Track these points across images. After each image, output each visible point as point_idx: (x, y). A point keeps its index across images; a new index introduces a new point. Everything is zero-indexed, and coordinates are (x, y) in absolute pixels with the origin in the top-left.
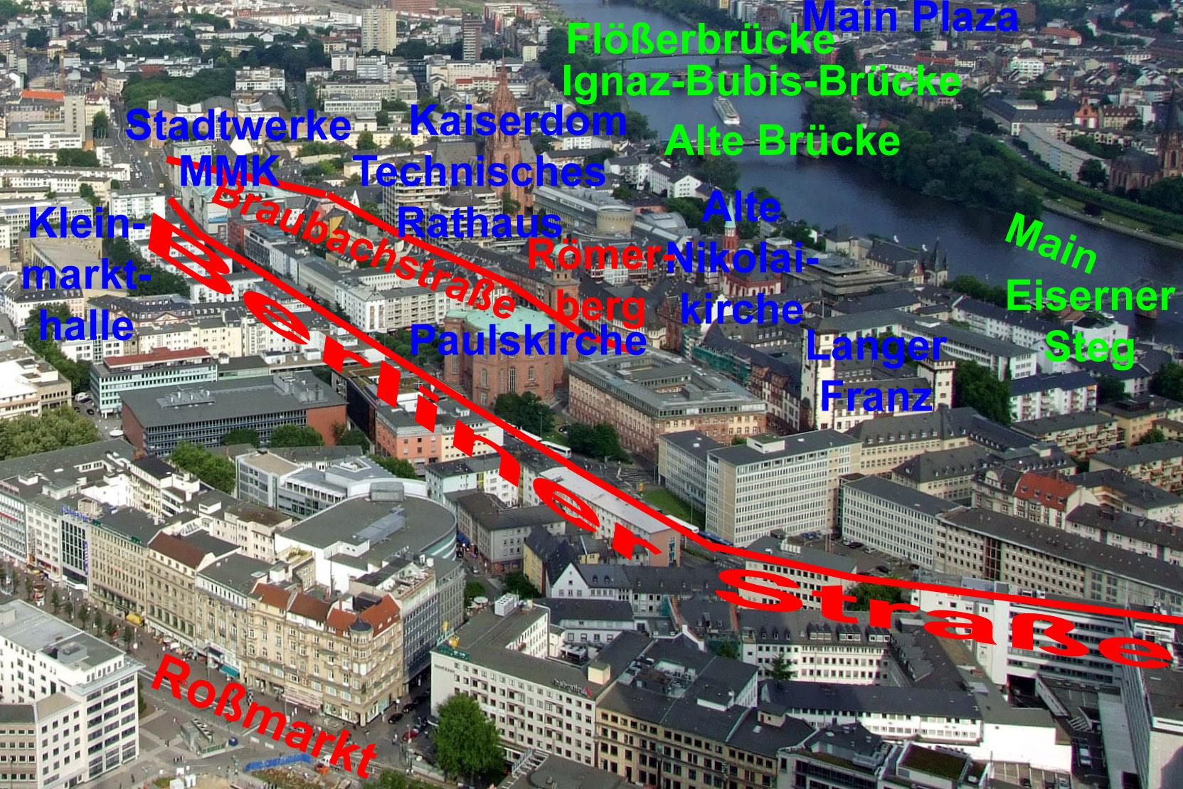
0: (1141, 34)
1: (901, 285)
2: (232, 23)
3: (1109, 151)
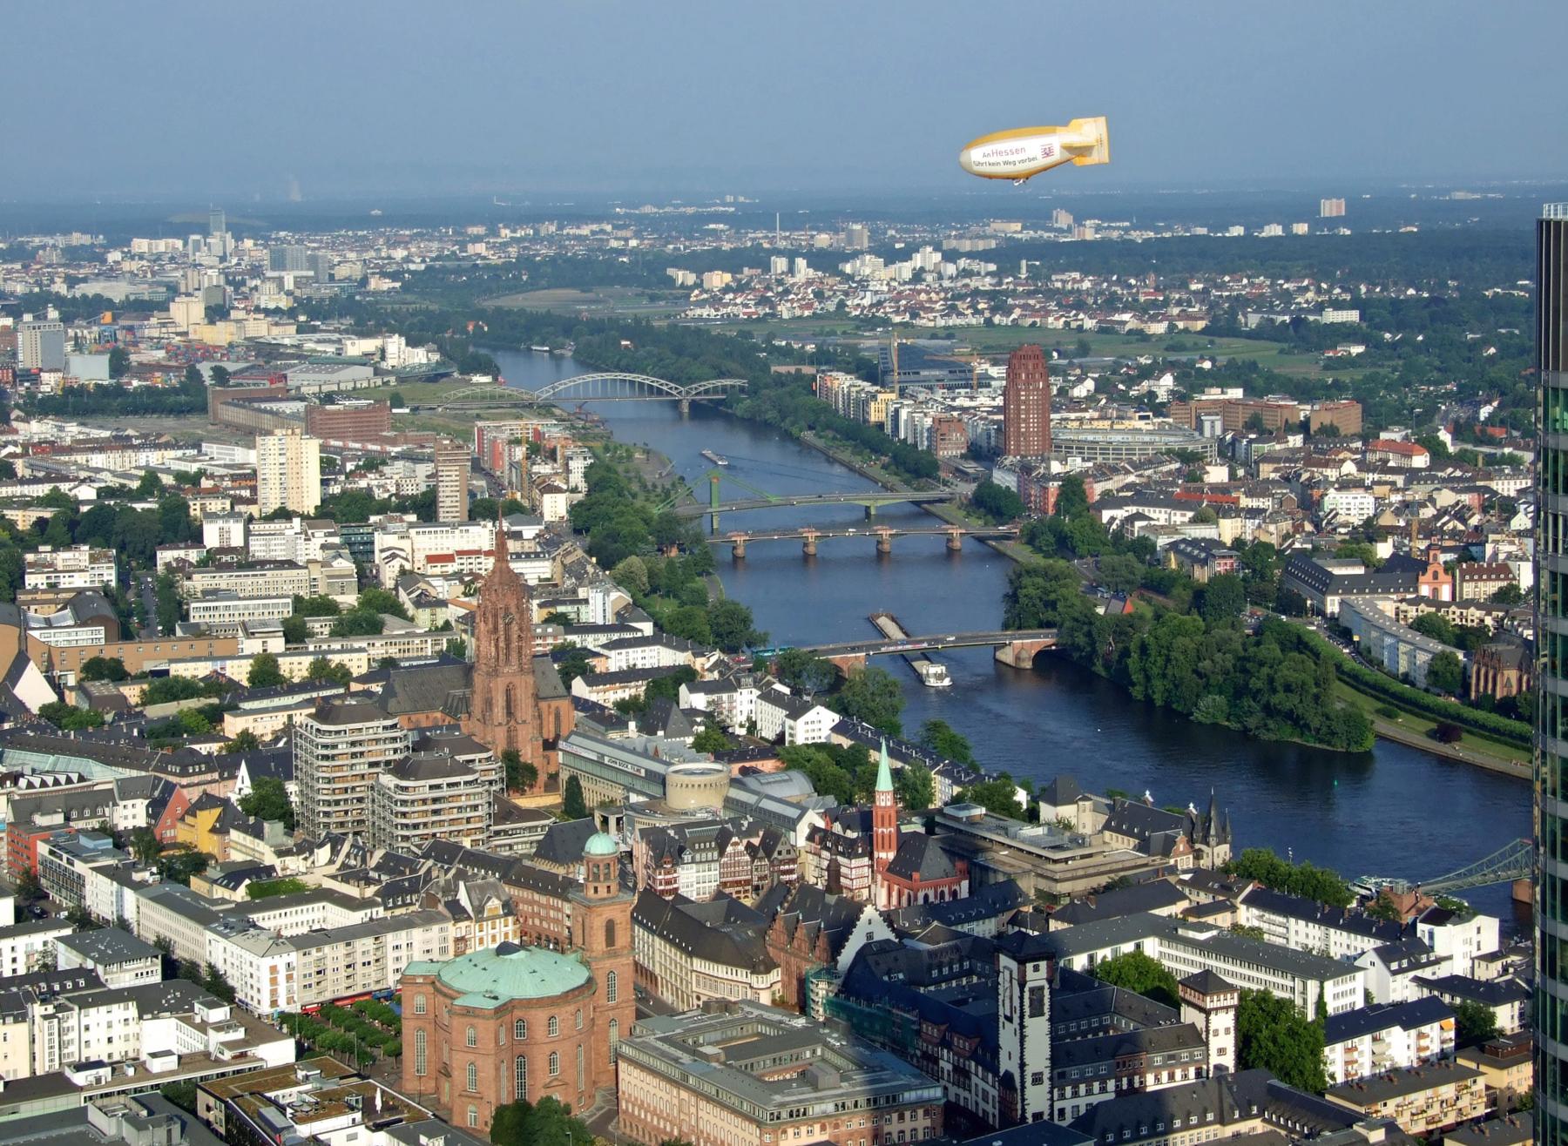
0: (1517, 447)
1: (1156, 872)
2: (20, 467)
3: (1465, 637)
